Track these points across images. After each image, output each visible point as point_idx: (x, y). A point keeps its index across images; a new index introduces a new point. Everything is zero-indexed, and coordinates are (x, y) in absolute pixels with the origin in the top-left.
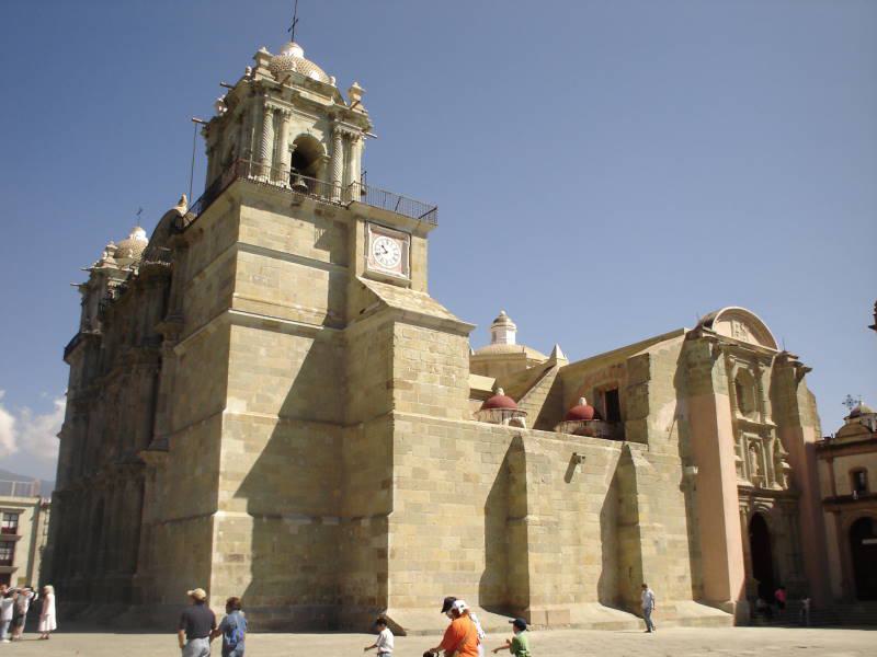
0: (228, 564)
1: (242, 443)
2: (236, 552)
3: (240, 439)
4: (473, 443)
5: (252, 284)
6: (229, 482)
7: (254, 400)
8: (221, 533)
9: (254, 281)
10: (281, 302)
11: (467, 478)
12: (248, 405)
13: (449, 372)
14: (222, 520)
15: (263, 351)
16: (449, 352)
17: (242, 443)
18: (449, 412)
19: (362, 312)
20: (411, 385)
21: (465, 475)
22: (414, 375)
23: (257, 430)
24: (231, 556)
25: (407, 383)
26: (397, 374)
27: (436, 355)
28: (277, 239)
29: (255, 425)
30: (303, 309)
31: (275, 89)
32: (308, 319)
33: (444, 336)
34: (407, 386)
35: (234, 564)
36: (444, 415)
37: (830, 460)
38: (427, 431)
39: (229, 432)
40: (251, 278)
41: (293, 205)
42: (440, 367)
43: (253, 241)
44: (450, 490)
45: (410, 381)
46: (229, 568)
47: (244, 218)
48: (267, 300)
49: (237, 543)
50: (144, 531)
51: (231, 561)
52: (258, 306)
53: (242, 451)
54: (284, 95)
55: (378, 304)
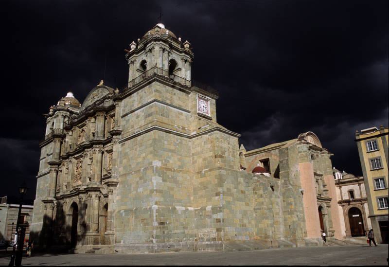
1: (161, 178)
7: (164, 161)
12: (162, 163)
13: (234, 152)
14: (157, 208)
15: (166, 142)
17: (161, 178)
19: (199, 129)
20: (223, 157)
23: (166, 173)
29: (165, 171)
35: (162, 226)
37: (340, 187)
46: (160, 228)
49: (162, 218)
50: (109, 215)
53: (161, 181)
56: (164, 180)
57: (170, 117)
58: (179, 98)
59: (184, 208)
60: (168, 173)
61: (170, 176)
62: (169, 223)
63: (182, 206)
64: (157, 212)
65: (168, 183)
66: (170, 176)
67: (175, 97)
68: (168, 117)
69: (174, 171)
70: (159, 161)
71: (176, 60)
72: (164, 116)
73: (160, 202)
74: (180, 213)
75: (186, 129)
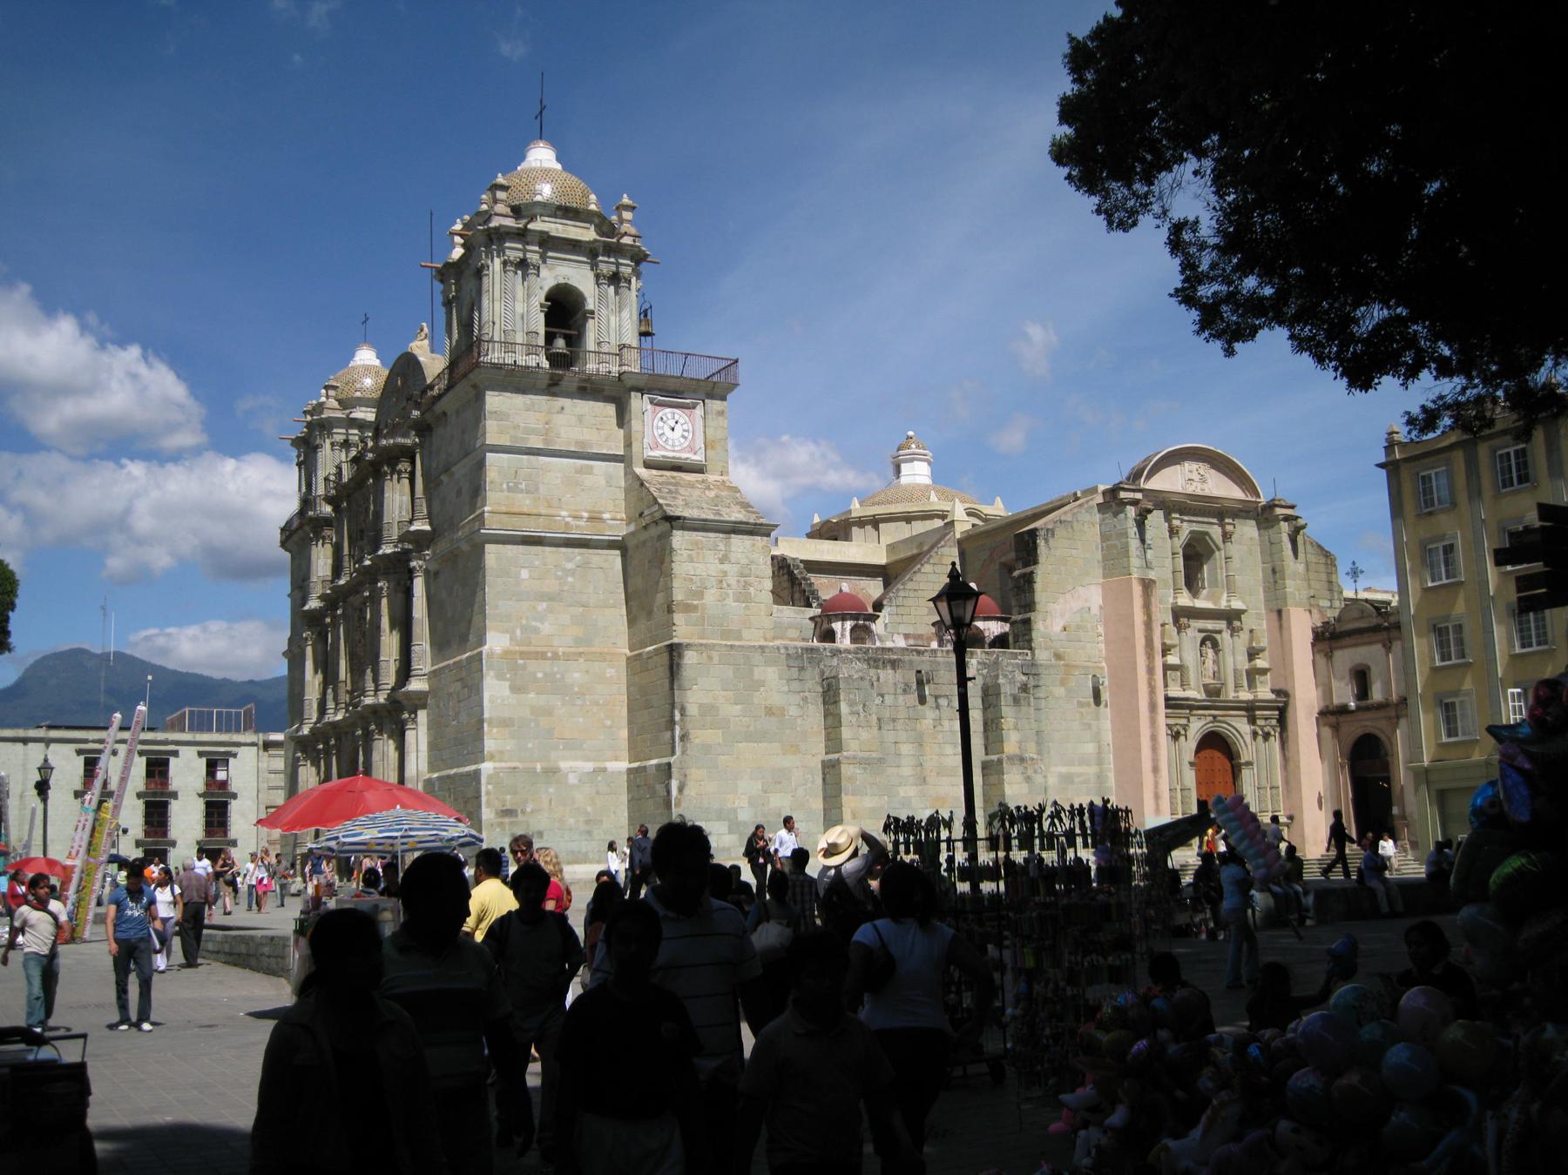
0: (500, 820)
1: (507, 683)
2: (508, 806)
3: (505, 679)
4: (774, 669)
5: (506, 493)
6: (495, 730)
7: (518, 632)
8: (490, 787)
9: (509, 489)
10: (543, 512)
11: (769, 711)
12: (511, 639)
13: (747, 585)
14: (491, 772)
15: (525, 574)
16: (746, 561)
17: (507, 683)
18: (746, 634)
19: (641, 515)
21: (766, 707)
22: (700, 594)
23: (524, 667)
24: (502, 811)
25: (692, 605)
26: (678, 595)
27: (726, 567)
28: (534, 432)
29: (520, 662)
30: (570, 516)
31: (518, 234)
32: (577, 527)
33: (736, 540)
34: (689, 608)
35: (507, 820)
36: (740, 639)
38: (716, 659)
39: (492, 673)
40: (505, 486)
41: (550, 385)
42: (733, 581)
43: (505, 441)
44: (748, 727)
45: (695, 602)
46: (501, 824)
47: (491, 413)
48: (525, 510)
49: (508, 797)
51: (503, 816)
52: (515, 519)
53: (507, 692)
54: (529, 238)
55: (657, 507)
56: (515, 689)
57: (542, 489)
58: (580, 418)
59: (589, 766)
60: (532, 665)
61: (540, 675)
62: (532, 812)
63: (587, 759)
64: (488, 783)
65: (532, 695)
66: (540, 675)
67: (559, 420)
68: (537, 490)
69: (556, 657)
70: (503, 632)
71: (574, 282)
72: (521, 491)
73: (501, 752)
74: (572, 779)
75: (606, 516)
